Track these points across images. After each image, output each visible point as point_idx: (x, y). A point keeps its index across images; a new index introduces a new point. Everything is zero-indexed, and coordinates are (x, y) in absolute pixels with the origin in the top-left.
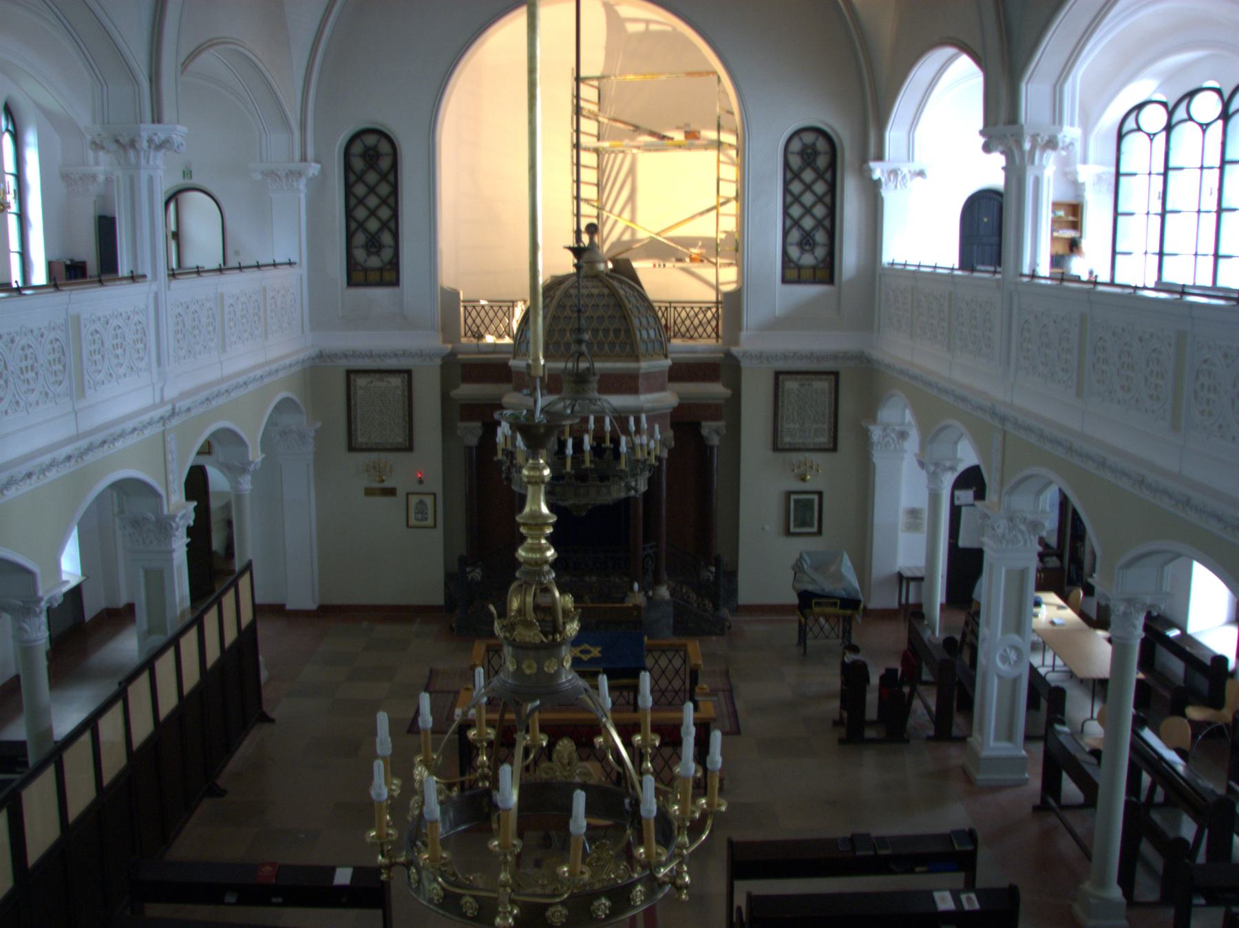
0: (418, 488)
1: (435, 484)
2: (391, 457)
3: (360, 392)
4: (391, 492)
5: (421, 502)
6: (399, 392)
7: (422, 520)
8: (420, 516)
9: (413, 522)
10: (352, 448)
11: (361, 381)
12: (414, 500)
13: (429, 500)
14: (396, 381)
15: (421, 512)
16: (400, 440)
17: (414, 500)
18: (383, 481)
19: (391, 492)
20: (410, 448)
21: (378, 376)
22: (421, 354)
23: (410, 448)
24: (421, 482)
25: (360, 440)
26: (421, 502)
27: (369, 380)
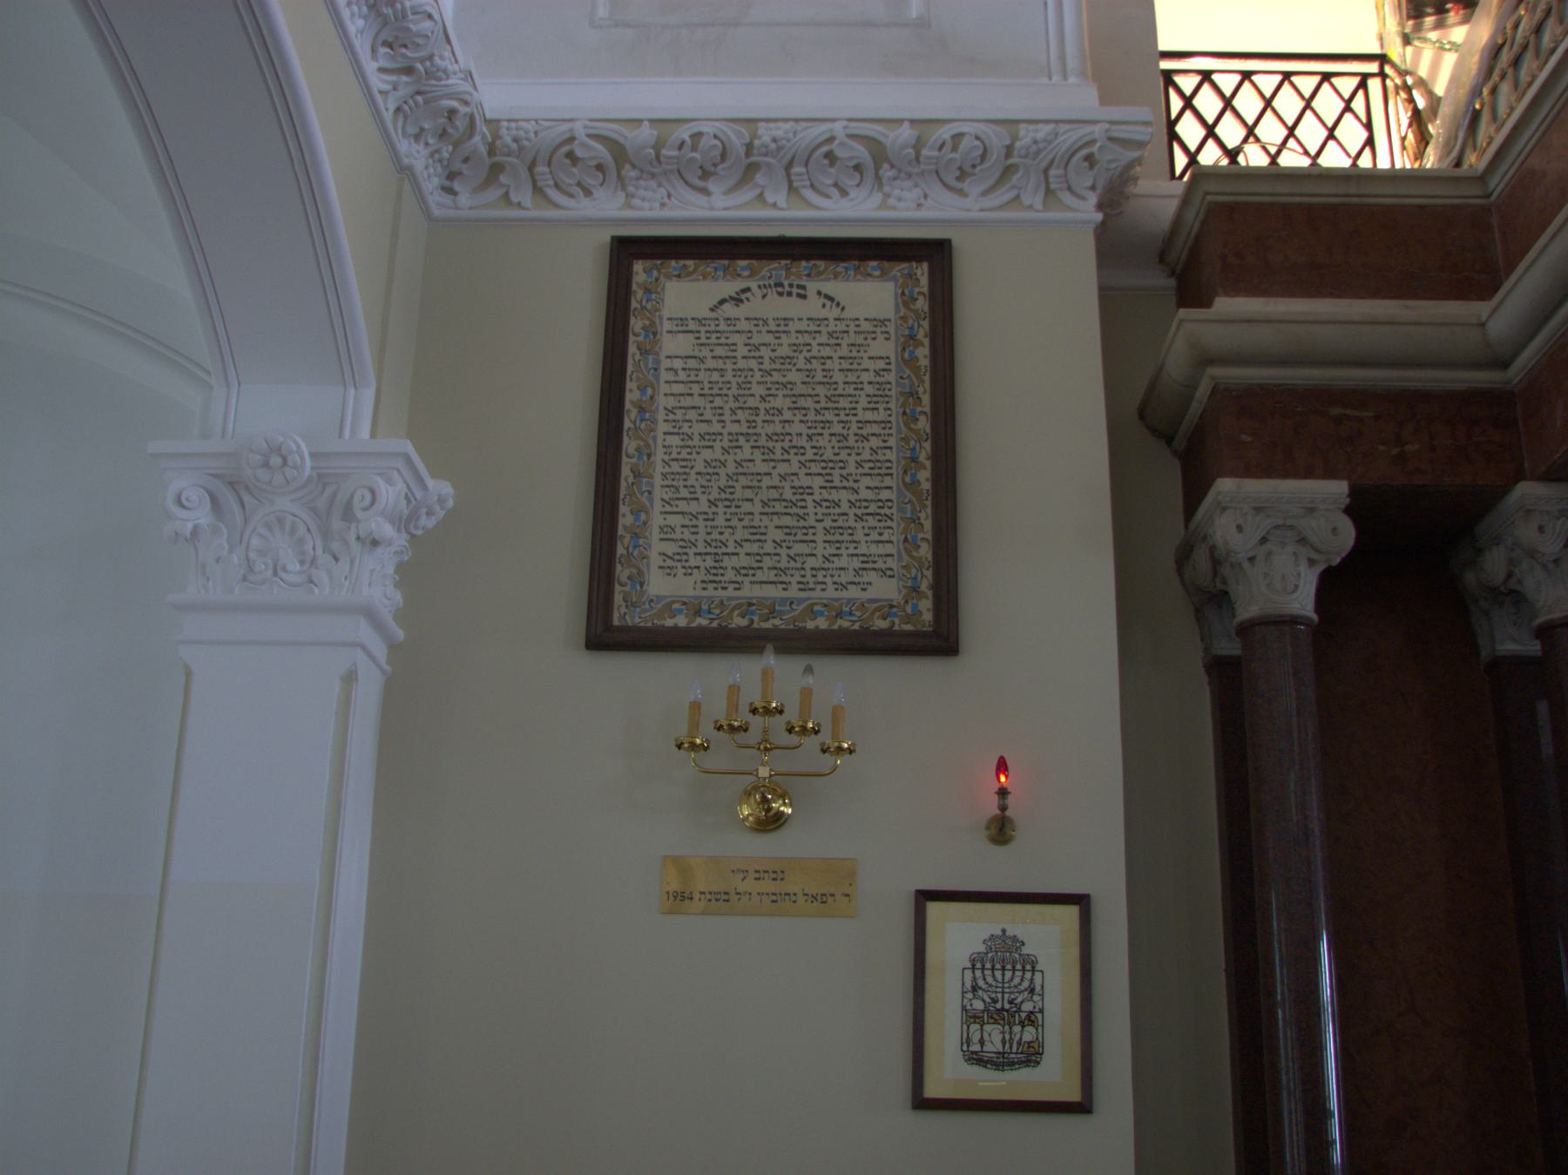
0: (999, 869)
1: (1083, 830)
2: (839, 682)
3: (674, 344)
4: (831, 891)
5: (1005, 954)
6: (884, 347)
7: (1001, 1062)
8: (994, 1037)
9: (949, 1072)
10: (605, 635)
11: (684, 296)
12: (958, 936)
13: (1047, 936)
14: (871, 296)
15: (1003, 1015)
16: (886, 589)
17: (958, 936)
18: (771, 822)
19: (831, 891)
20: (940, 640)
21: (774, 269)
22: (997, 159)
23: (940, 640)
24: (1001, 830)
25: (658, 585)
26: (1005, 954)
27: (730, 287)
